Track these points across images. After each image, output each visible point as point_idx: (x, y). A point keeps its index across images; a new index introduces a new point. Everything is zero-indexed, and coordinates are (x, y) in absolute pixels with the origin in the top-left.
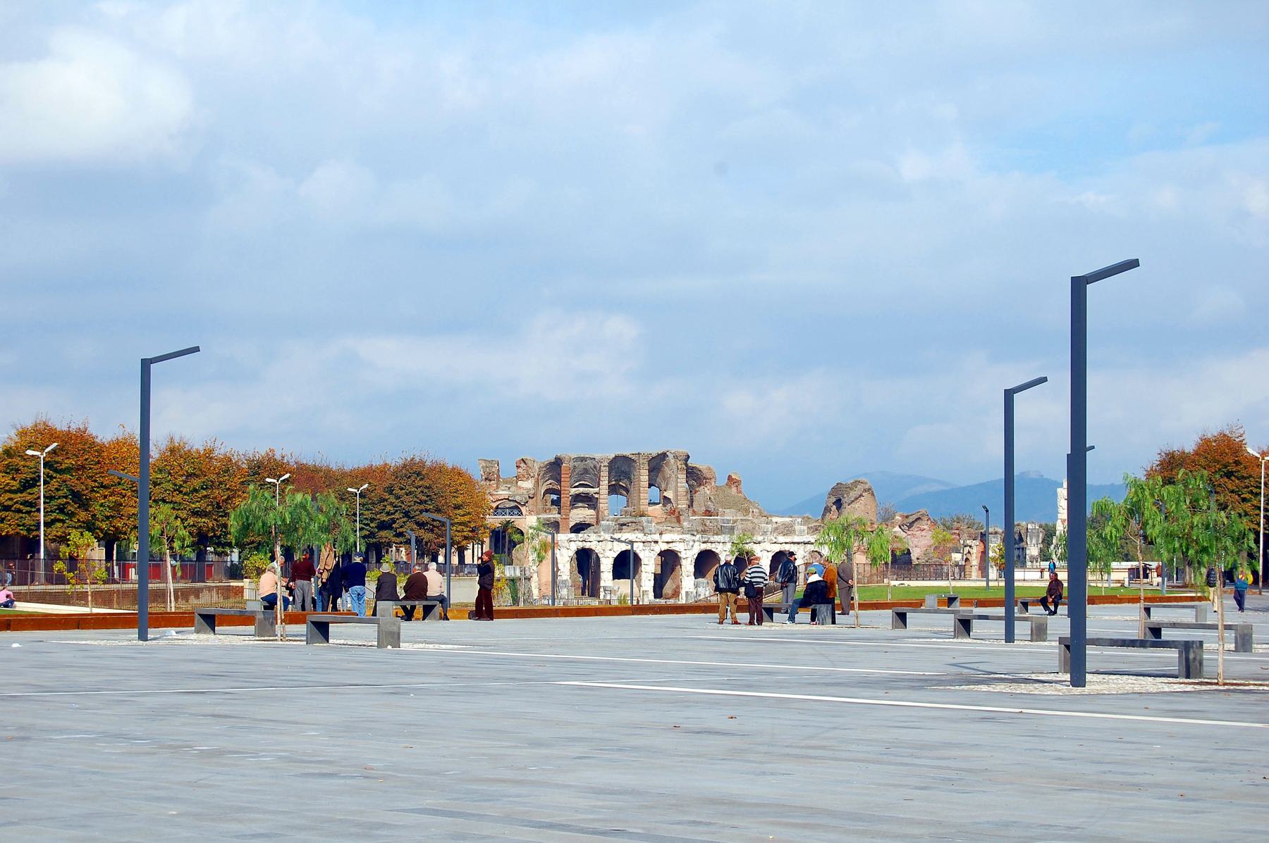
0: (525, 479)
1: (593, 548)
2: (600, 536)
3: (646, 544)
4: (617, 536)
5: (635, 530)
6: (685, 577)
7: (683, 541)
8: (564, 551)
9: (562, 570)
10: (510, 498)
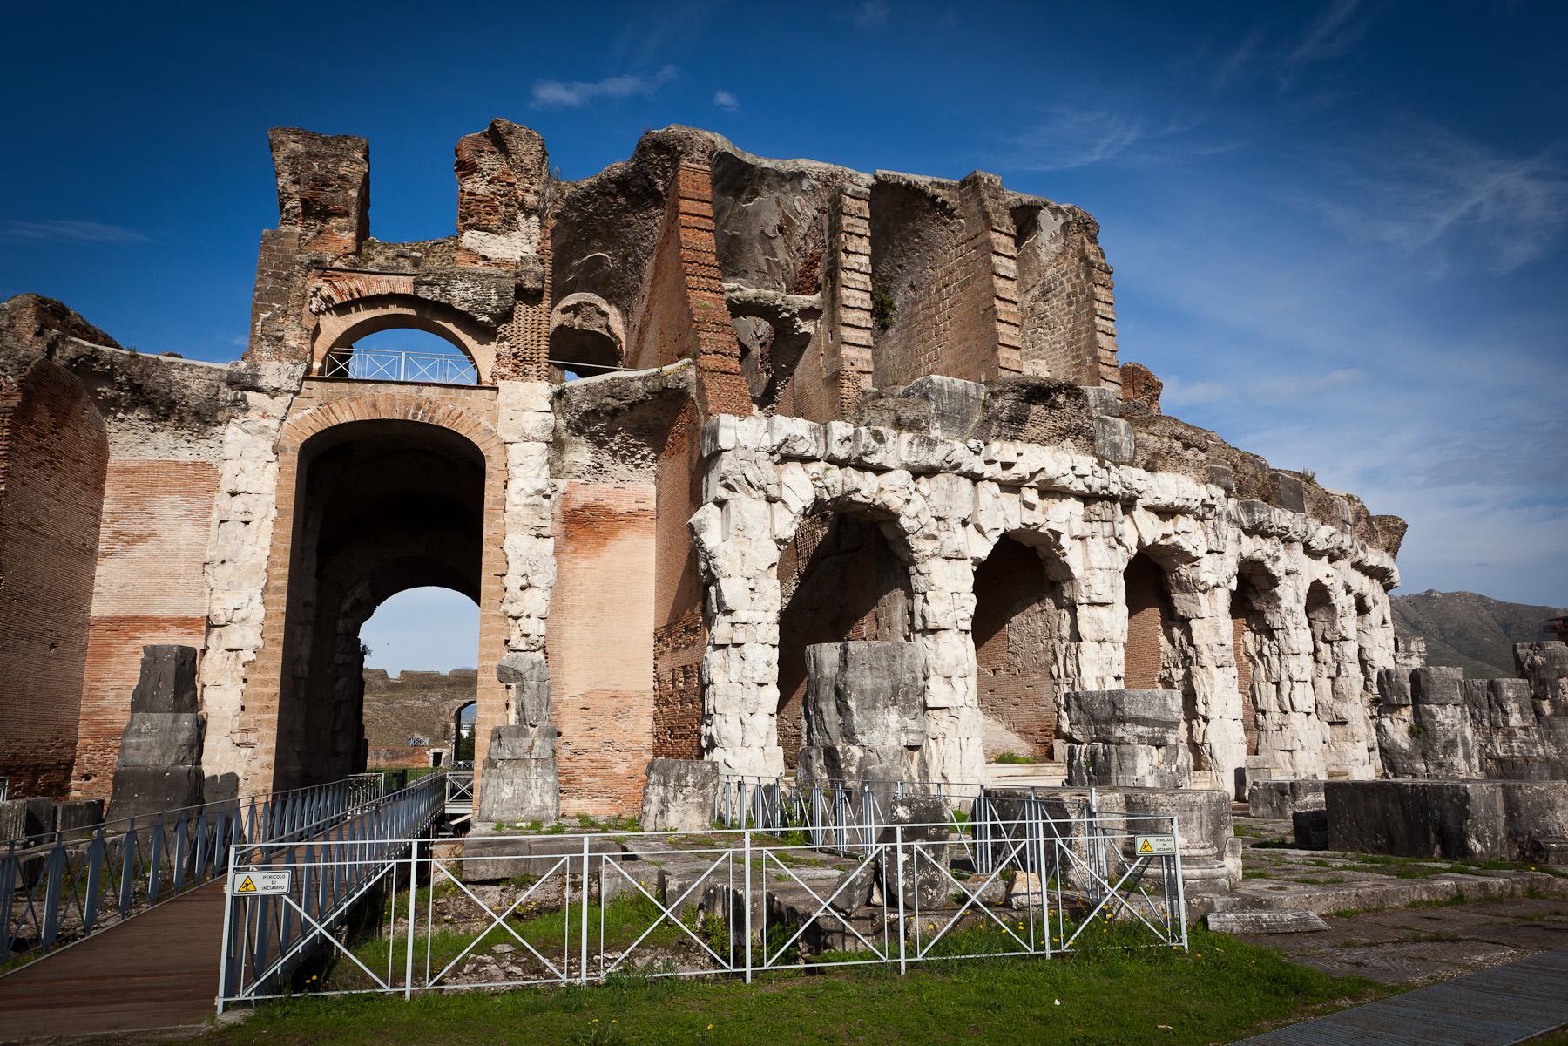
0: (495, 221)
1: (895, 502)
2: (931, 444)
3: (1097, 507)
4: (1002, 450)
5: (1065, 434)
6: (1212, 668)
7: (1206, 511)
8: (748, 507)
9: (741, 615)
10: (423, 292)
